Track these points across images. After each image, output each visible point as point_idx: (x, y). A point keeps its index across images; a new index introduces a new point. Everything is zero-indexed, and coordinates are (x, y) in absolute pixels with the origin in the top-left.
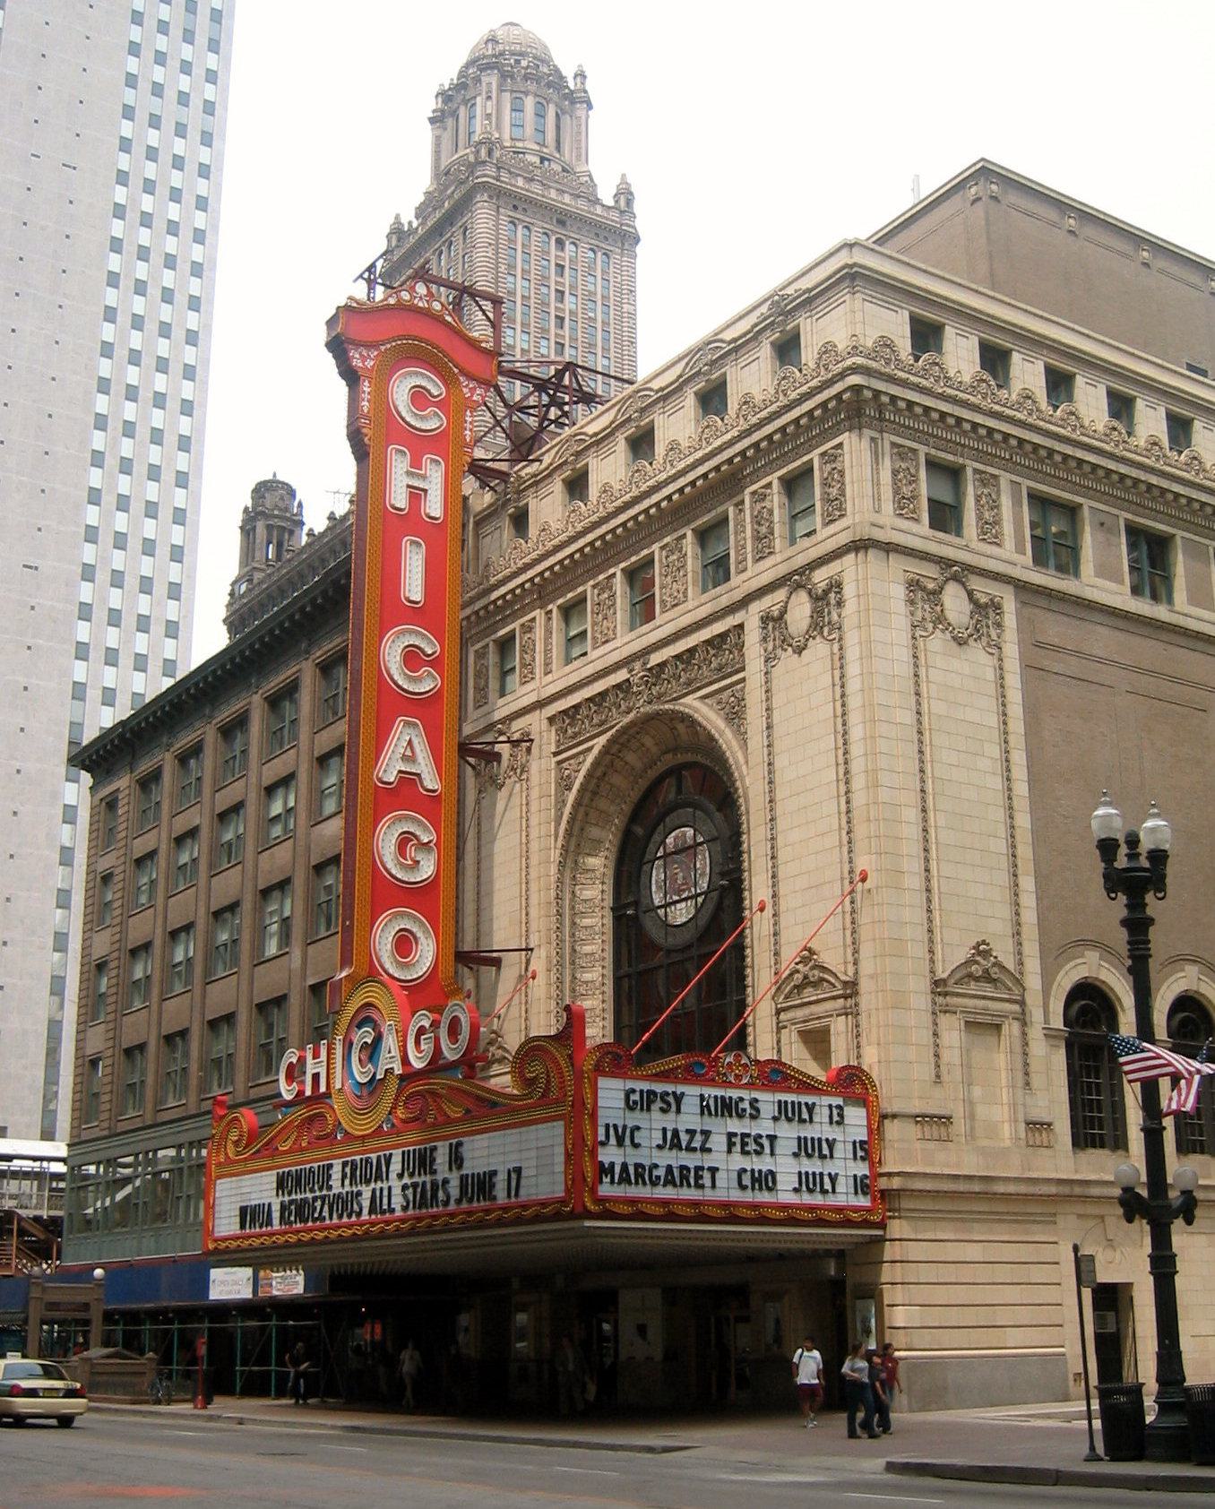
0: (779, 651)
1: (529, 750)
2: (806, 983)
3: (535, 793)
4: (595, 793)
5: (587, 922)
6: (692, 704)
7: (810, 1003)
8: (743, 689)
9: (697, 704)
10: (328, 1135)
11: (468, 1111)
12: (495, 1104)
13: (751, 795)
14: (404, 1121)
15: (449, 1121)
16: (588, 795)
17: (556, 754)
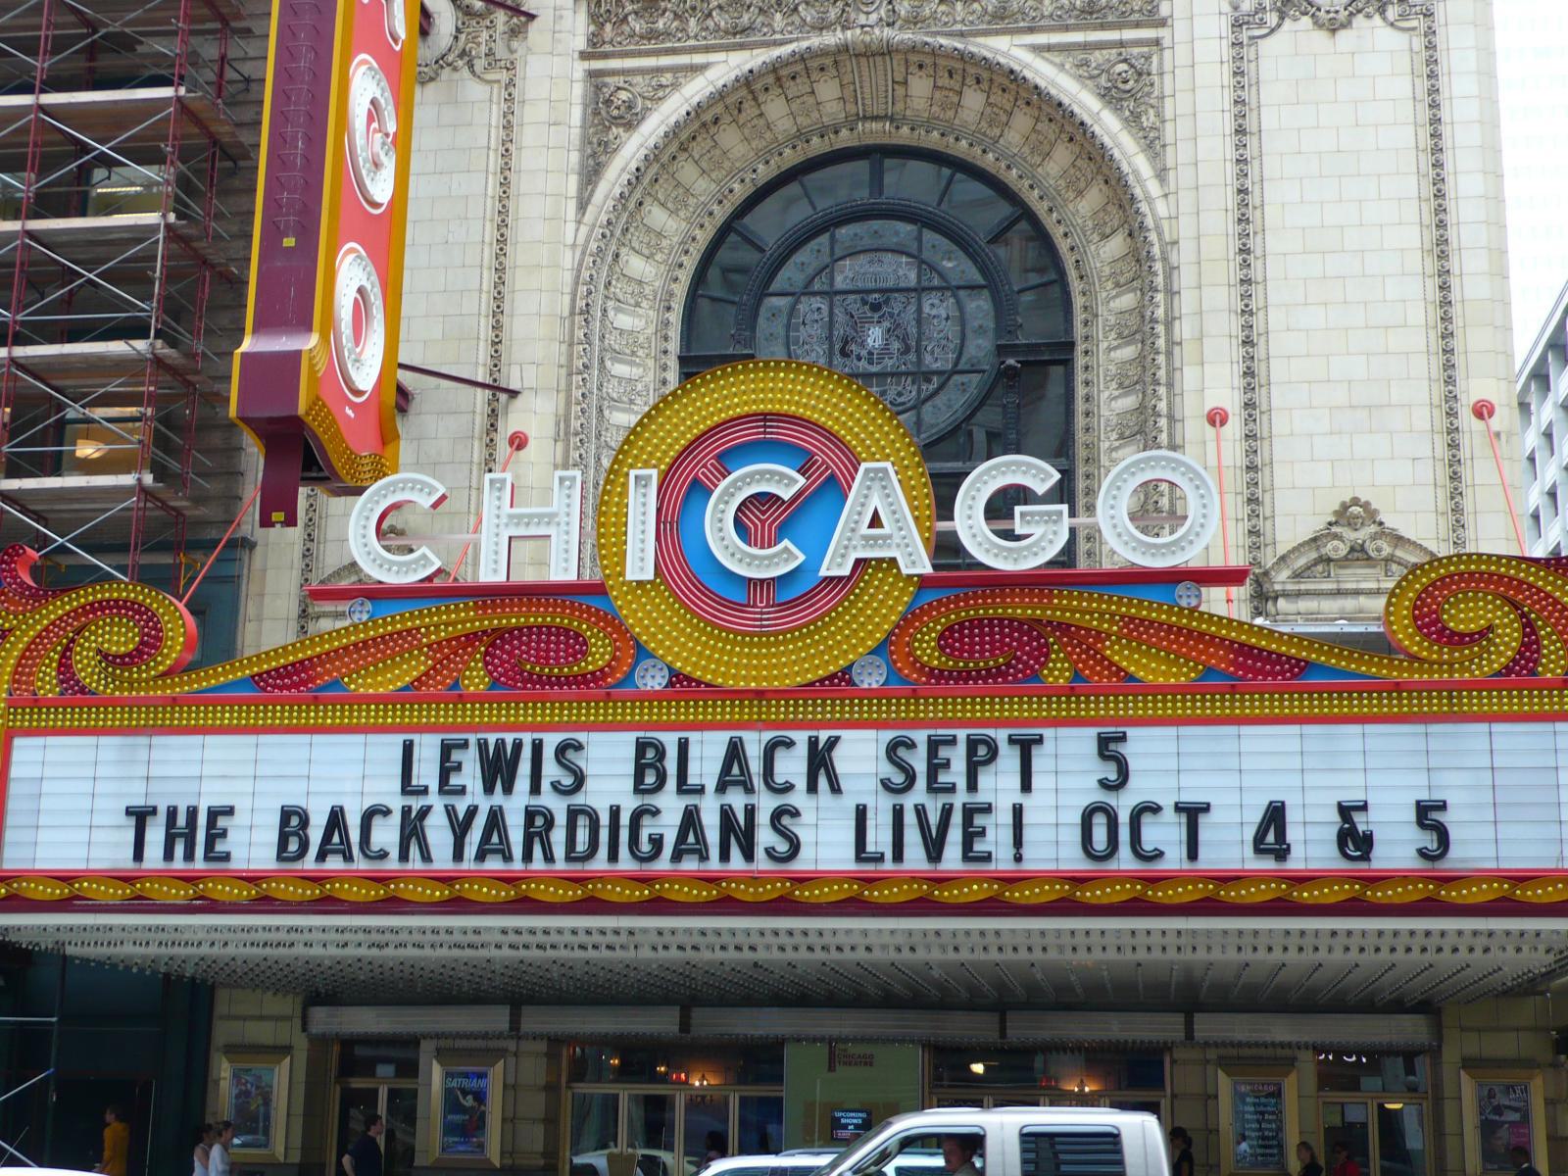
0: (1272, 19)
1: (514, 33)
2: (1358, 554)
3: (532, 116)
4: (683, 148)
5: (620, 369)
6: (1008, 49)
7: (1357, 593)
8: (1148, 58)
9: (1027, 57)
10: (582, 680)
11: (1209, 671)
12: (1302, 667)
13: (1186, 229)
14: (939, 675)
15: (1128, 684)
16: (673, 148)
17: (584, 56)
